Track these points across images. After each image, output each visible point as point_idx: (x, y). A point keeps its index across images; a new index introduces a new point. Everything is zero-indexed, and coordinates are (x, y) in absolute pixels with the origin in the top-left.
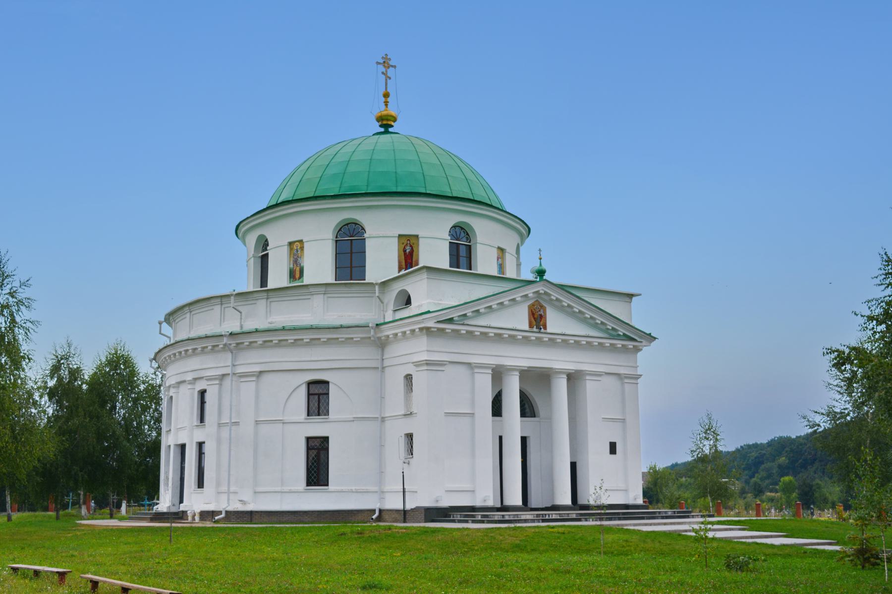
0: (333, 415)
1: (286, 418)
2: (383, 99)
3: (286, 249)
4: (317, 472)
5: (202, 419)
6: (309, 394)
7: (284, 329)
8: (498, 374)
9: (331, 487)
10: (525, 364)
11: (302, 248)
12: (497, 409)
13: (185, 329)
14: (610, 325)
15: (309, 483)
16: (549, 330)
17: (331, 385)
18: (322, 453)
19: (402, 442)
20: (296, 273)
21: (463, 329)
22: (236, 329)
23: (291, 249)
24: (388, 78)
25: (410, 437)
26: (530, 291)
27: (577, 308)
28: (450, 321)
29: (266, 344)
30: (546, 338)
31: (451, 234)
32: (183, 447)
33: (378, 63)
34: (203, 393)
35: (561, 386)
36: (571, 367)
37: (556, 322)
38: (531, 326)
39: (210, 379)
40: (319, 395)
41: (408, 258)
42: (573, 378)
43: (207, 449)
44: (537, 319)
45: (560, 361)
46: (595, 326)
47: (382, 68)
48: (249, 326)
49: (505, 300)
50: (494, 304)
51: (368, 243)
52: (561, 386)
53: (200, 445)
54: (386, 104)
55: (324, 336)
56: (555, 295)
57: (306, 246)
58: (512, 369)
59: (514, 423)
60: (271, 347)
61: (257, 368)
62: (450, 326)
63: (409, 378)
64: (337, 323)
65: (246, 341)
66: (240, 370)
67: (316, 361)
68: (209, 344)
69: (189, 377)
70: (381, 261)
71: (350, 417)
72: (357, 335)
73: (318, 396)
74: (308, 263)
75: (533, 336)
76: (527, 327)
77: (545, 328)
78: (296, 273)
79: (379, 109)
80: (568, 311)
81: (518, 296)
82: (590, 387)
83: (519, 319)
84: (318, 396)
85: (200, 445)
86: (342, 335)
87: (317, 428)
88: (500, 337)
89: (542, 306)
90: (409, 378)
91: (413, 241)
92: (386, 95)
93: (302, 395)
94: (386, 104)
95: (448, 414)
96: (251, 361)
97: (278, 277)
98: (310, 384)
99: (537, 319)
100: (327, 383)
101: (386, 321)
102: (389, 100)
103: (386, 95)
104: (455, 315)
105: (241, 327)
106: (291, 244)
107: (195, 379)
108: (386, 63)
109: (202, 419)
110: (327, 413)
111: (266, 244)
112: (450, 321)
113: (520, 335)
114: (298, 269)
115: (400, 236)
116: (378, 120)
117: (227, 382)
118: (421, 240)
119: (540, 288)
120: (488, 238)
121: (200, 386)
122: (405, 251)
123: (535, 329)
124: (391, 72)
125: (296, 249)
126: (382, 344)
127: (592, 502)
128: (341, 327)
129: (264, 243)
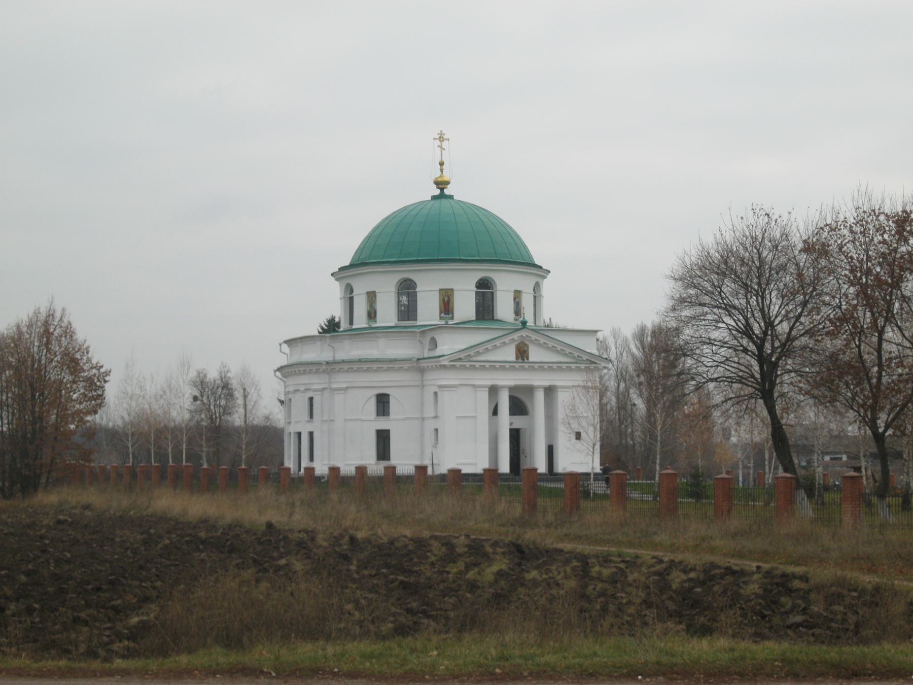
0: (392, 416)
1: (363, 418)
4: (383, 451)
5: (311, 416)
7: (360, 361)
8: (494, 391)
10: (512, 383)
11: (375, 297)
16: (531, 359)
17: (391, 397)
19: (433, 433)
20: (372, 315)
21: (468, 364)
22: (330, 359)
23: (368, 297)
24: (442, 149)
25: (436, 430)
26: (516, 336)
27: (550, 344)
28: (460, 359)
29: (350, 370)
30: (526, 366)
31: (477, 287)
32: (299, 434)
33: (435, 139)
34: (311, 399)
35: (540, 397)
37: (535, 354)
38: (517, 358)
39: (315, 390)
41: (447, 307)
42: (550, 391)
44: (522, 353)
45: (539, 380)
48: (340, 356)
51: (419, 295)
52: (540, 397)
53: (311, 434)
54: (442, 171)
56: (534, 336)
57: (378, 295)
58: (503, 387)
59: (505, 420)
61: (344, 385)
62: (463, 361)
63: (436, 393)
64: (394, 357)
65: (337, 367)
66: (335, 386)
67: (383, 381)
68: (314, 368)
69: (302, 388)
70: (428, 310)
72: (406, 366)
73: (383, 403)
74: (380, 307)
75: (517, 365)
76: (513, 358)
77: (528, 358)
78: (372, 315)
80: (544, 346)
81: (507, 340)
82: (563, 398)
83: (509, 354)
84: (383, 403)
85: (311, 434)
86: (397, 366)
87: (383, 424)
88: (494, 367)
89: (526, 345)
90: (436, 393)
92: (442, 164)
93: (373, 402)
94: (442, 171)
95: (458, 417)
96: (341, 380)
97: (360, 320)
99: (522, 353)
101: (426, 356)
102: (444, 167)
103: (442, 164)
104: (462, 356)
106: (368, 293)
108: (441, 138)
109: (311, 416)
110: (388, 414)
111: (352, 291)
112: (460, 359)
113: (507, 365)
115: (441, 290)
117: (326, 393)
119: (524, 333)
120: (506, 284)
121: (310, 394)
123: (520, 360)
125: (372, 297)
126: (422, 371)
128: (396, 360)
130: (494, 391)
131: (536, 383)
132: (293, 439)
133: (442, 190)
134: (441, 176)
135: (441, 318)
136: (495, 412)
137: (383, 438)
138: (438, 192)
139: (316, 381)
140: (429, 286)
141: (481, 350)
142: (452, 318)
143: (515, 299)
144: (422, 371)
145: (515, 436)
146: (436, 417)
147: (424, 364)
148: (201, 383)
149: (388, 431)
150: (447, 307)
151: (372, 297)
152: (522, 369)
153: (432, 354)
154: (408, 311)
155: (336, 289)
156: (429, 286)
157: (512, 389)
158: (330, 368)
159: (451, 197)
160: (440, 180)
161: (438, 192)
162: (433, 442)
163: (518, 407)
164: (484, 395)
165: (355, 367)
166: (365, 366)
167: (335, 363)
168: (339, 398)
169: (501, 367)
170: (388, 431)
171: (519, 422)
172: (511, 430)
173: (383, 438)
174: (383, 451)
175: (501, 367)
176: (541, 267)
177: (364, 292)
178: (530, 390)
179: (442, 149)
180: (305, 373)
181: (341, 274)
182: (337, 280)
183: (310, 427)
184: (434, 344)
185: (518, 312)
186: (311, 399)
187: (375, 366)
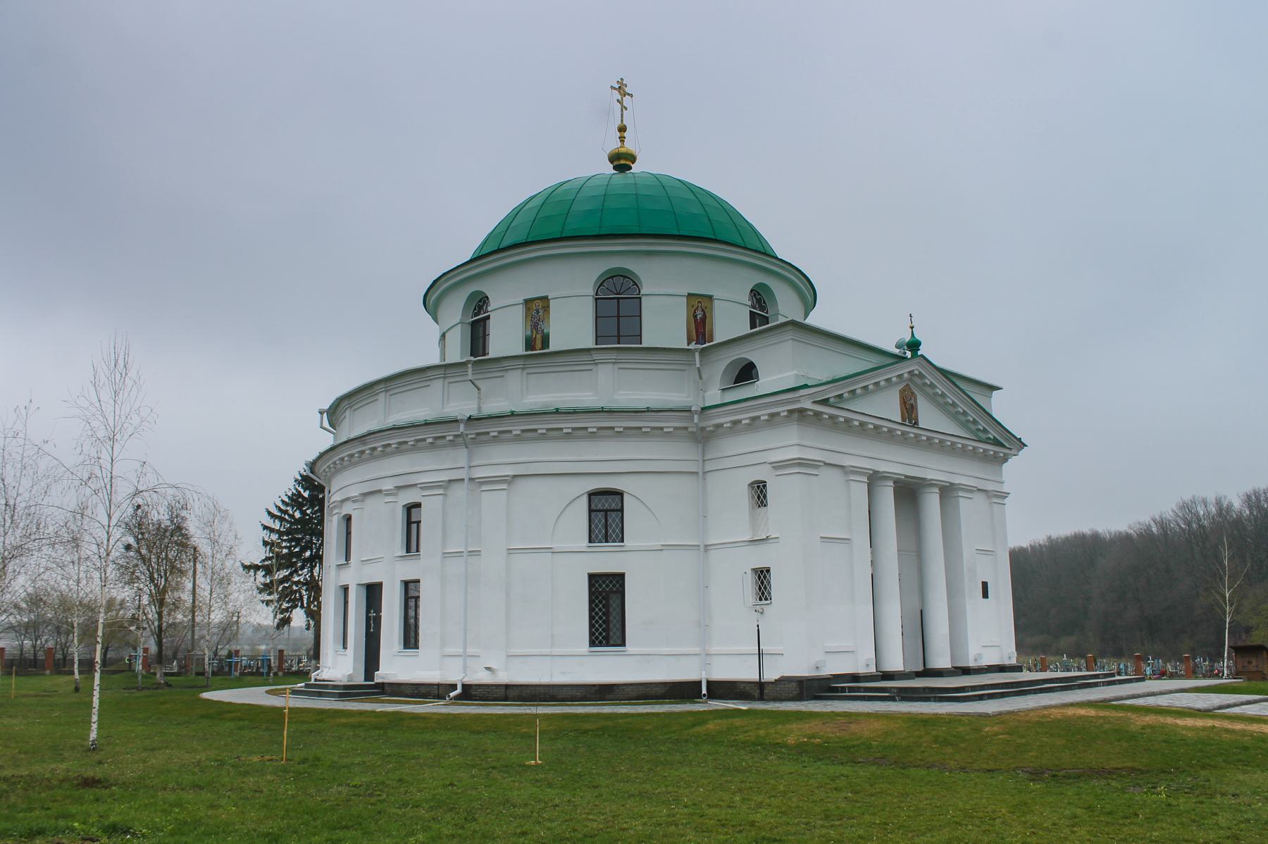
1: (556, 546)
2: (618, 134)
3: (520, 311)
6: (591, 511)
9: (630, 647)
11: (546, 308)
13: (359, 423)
14: (982, 424)
15: (592, 644)
17: (626, 497)
18: (614, 601)
19: (750, 583)
22: (474, 413)
23: (528, 310)
24: (624, 108)
26: (904, 369)
38: (903, 419)
40: (606, 511)
42: (947, 491)
43: (426, 593)
45: (932, 468)
46: (964, 425)
47: (617, 95)
48: (495, 405)
49: (881, 379)
53: (410, 590)
54: (622, 139)
55: (619, 424)
60: (509, 440)
61: (510, 471)
64: (643, 406)
66: (479, 473)
67: (605, 460)
68: (429, 435)
69: (388, 485)
71: (656, 544)
72: (669, 424)
73: (606, 515)
79: (613, 145)
81: (893, 375)
83: (887, 407)
84: (606, 515)
85: (410, 590)
86: (646, 423)
87: (606, 560)
92: (622, 129)
93: (581, 511)
94: (622, 139)
96: (499, 459)
98: (592, 495)
100: (620, 494)
102: (625, 134)
103: (622, 129)
105: (479, 409)
106: (528, 302)
107: (366, 495)
108: (621, 88)
114: (539, 337)
115: (690, 295)
116: (611, 161)
117: (459, 492)
118: (716, 302)
119: (915, 367)
122: (695, 317)
124: (627, 99)
125: (537, 309)
127: (972, 664)
128: (648, 410)
129: (479, 303)
131: (930, 475)
137: (606, 597)
139: (429, 466)
149: (621, 577)
151: (537, 309)
152: (904, 440)
166: (567, 425)
168: (492, 500)
170: (621, 577)
173: (606, 597)
179: (624, 108)
183: (408, 570)
186: (411, 508)
187: (592, 424)
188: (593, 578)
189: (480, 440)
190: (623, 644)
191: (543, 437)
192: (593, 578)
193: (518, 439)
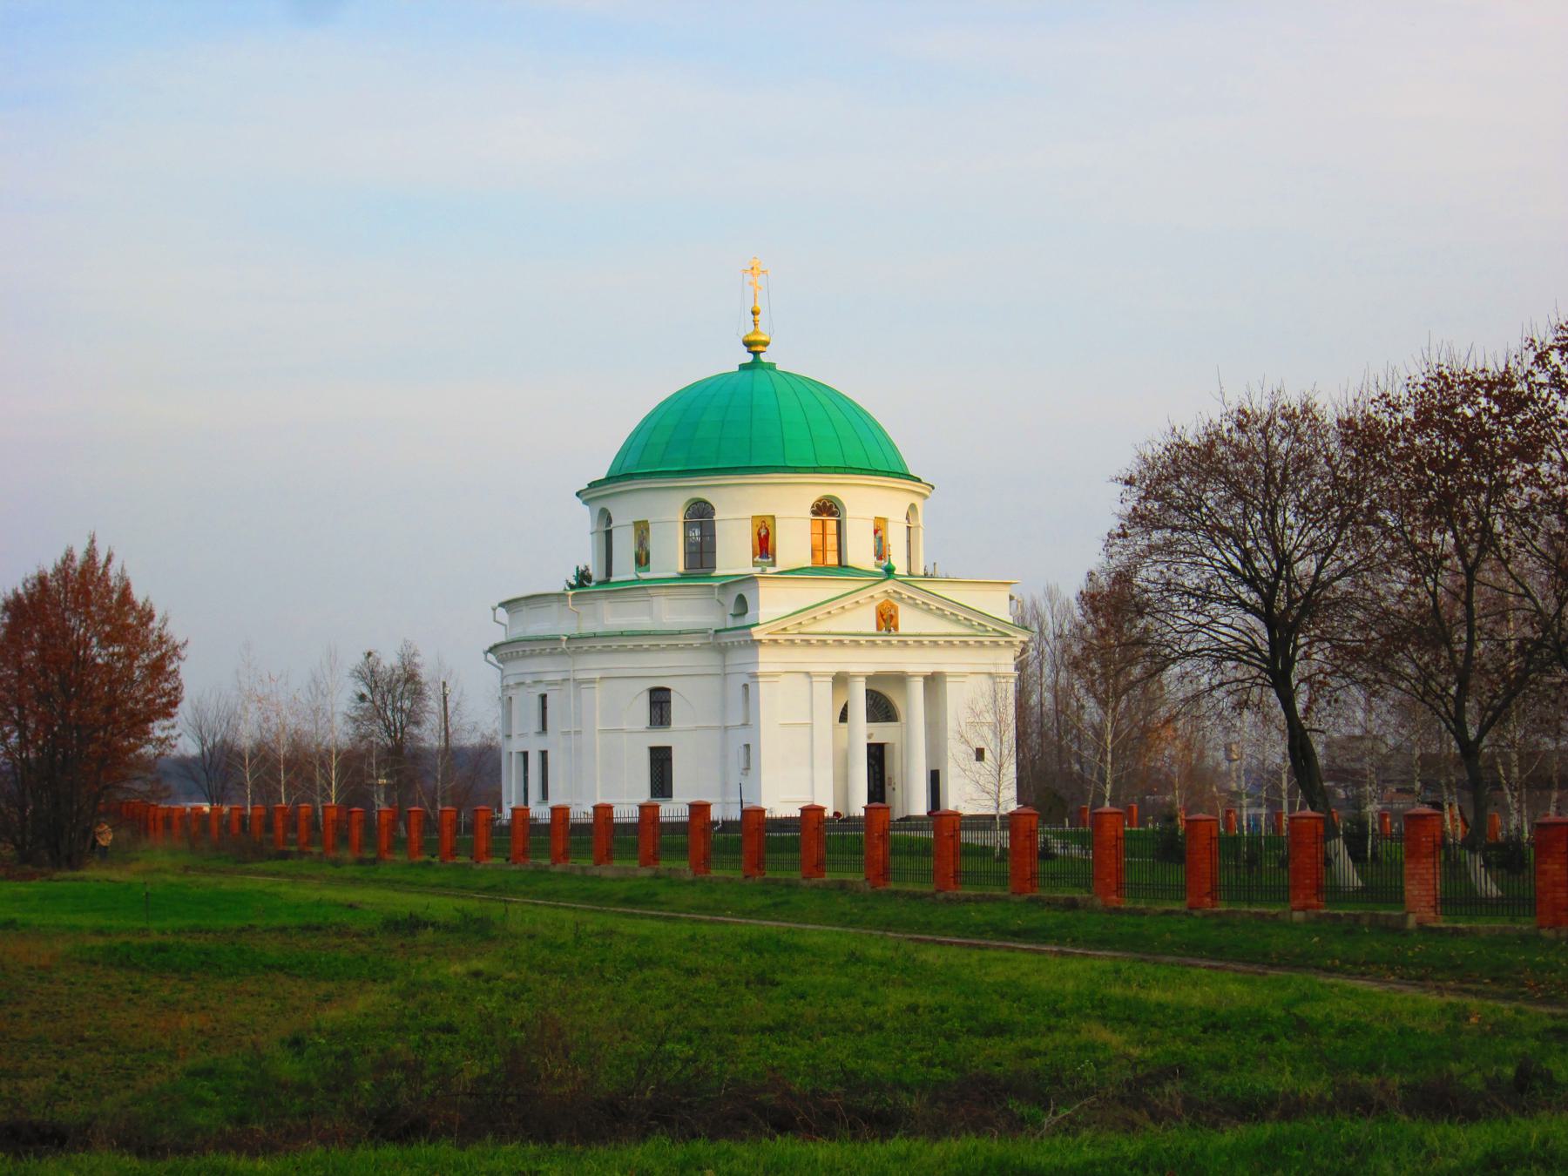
3: (632, 530)
4: (661, 782)
7: (622, 634)
8: (841, 681)
9: (675, 798)
10: (871, 669)
12: (844, 717)
16: (901, 630)
19: (742, 751)
20: (642, 560)
25: (747, 746)
26: (878, 591)
29: (607, 650)
30: (894, 640)
31: (814, 513)
32: (525, 754)
34: (544, 697)
35: (917, 689)
36: (929, 670)
37: (908, 621)
38: (879, 628)
41: (764, 546)
42: (933, 681)
44: (887, 619)
45: (916, 663)
46: (958, 621)
48: (588, 627)
49: (847, 602)
50: (834, 608)
53: (544, 754)
55: (663, 642)
56: (906, 593)
59: (862, 731)
63: (746, 686)
65: (585, 645)
67: (661, 667)
68: (547, 647)
69: (529, 680)
72: (696, 642)
73: (660, 702)
75: (878, 640)
76: (873, 629)
77: (896, 628)
78: (642, 560)
79: (747, 330)
81: (861, 597)
83: (866, 621)
84: (660, 702)
85: (544, 754)
86: (681, 642)
87: (660, 739)
90: (746, 686)
91: (769, 522)
96: (592, 666)
97: (624, 568)
99: (887, 619)
100: (668, 690)
101: (729, 626)
111: (609, 521)
119: (889, 586)
121: (542, 690)
125: (642, 529)
126: (723, 650)
128: (680, 633)
130: (841, 681)
132: (516, 763)
133: (756, 353)
134: (755, 332)
135: (755, 564)
136: (844, 717)
137: (661, 760)
138: (749, 358)
139: (549, 669)
140: (737, 508)
141: (819, 613)
142: (774, 564)
143: (876, 532)
144: (723, 650)
145: (877, 754)
146: (745, 725)
147: (726, 639)
148: (370, 674)
150: (764, 546)
151: (642, 529)
153: (739, 623)
154: (701, 555)
155: (583, 517)
156: (737, 508)
157: (870, 679)
158: (573, 646)
159: (771, 366)
160: (752, 338)
161: (749, 358)
162: (743, 765)
163: (881, 708)
164: (824, 688)
165: (615, 644)
167: (582, 638)
169: (854, 641)
171: (884, 733)
172: (869, 745)
173: (661, 760)
174: (661, 782)
175: (854, 641)
176: (919, 480)
177: (630, 522)
178: (901, 679)
180: (532, 655)
181: (592, 492)
182: (586, 502)
184: (742, 605)
185: (880, 554)
187: (646, 643)
188: (653, 750)
189: (578, 652)
190: (670, 796)
191: (616, 651)
192: (653, 750)
193: (600, 652)
